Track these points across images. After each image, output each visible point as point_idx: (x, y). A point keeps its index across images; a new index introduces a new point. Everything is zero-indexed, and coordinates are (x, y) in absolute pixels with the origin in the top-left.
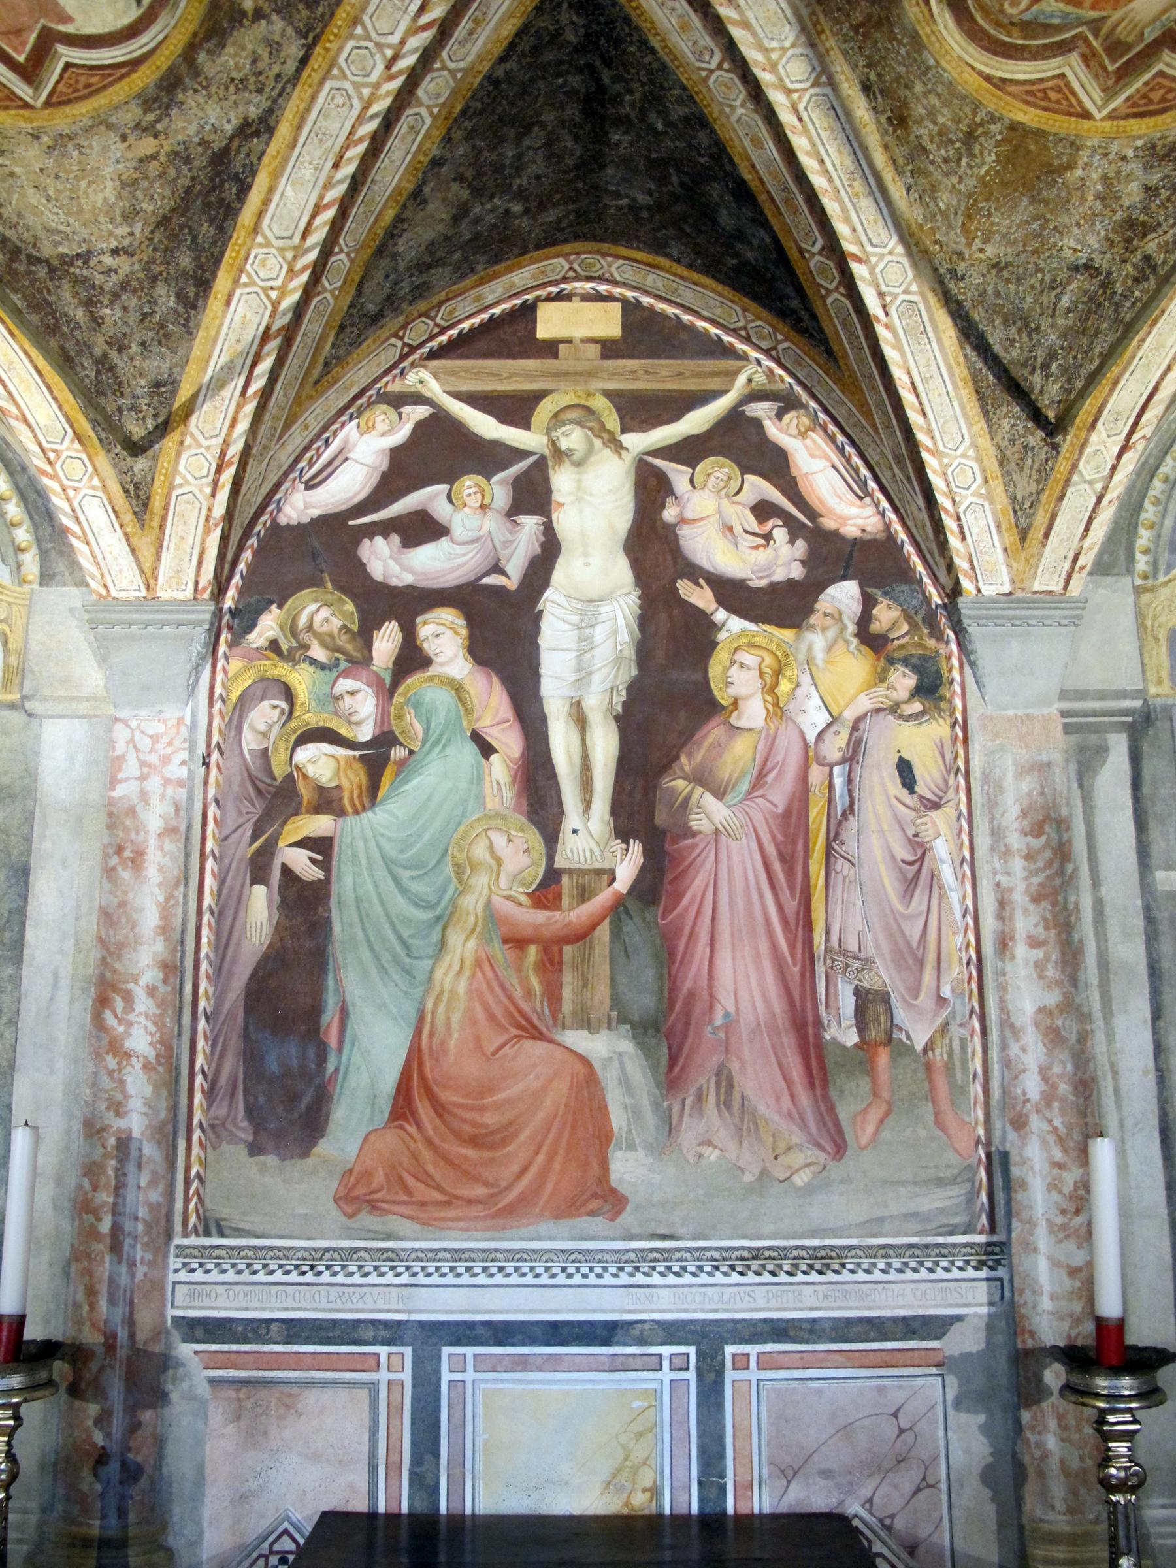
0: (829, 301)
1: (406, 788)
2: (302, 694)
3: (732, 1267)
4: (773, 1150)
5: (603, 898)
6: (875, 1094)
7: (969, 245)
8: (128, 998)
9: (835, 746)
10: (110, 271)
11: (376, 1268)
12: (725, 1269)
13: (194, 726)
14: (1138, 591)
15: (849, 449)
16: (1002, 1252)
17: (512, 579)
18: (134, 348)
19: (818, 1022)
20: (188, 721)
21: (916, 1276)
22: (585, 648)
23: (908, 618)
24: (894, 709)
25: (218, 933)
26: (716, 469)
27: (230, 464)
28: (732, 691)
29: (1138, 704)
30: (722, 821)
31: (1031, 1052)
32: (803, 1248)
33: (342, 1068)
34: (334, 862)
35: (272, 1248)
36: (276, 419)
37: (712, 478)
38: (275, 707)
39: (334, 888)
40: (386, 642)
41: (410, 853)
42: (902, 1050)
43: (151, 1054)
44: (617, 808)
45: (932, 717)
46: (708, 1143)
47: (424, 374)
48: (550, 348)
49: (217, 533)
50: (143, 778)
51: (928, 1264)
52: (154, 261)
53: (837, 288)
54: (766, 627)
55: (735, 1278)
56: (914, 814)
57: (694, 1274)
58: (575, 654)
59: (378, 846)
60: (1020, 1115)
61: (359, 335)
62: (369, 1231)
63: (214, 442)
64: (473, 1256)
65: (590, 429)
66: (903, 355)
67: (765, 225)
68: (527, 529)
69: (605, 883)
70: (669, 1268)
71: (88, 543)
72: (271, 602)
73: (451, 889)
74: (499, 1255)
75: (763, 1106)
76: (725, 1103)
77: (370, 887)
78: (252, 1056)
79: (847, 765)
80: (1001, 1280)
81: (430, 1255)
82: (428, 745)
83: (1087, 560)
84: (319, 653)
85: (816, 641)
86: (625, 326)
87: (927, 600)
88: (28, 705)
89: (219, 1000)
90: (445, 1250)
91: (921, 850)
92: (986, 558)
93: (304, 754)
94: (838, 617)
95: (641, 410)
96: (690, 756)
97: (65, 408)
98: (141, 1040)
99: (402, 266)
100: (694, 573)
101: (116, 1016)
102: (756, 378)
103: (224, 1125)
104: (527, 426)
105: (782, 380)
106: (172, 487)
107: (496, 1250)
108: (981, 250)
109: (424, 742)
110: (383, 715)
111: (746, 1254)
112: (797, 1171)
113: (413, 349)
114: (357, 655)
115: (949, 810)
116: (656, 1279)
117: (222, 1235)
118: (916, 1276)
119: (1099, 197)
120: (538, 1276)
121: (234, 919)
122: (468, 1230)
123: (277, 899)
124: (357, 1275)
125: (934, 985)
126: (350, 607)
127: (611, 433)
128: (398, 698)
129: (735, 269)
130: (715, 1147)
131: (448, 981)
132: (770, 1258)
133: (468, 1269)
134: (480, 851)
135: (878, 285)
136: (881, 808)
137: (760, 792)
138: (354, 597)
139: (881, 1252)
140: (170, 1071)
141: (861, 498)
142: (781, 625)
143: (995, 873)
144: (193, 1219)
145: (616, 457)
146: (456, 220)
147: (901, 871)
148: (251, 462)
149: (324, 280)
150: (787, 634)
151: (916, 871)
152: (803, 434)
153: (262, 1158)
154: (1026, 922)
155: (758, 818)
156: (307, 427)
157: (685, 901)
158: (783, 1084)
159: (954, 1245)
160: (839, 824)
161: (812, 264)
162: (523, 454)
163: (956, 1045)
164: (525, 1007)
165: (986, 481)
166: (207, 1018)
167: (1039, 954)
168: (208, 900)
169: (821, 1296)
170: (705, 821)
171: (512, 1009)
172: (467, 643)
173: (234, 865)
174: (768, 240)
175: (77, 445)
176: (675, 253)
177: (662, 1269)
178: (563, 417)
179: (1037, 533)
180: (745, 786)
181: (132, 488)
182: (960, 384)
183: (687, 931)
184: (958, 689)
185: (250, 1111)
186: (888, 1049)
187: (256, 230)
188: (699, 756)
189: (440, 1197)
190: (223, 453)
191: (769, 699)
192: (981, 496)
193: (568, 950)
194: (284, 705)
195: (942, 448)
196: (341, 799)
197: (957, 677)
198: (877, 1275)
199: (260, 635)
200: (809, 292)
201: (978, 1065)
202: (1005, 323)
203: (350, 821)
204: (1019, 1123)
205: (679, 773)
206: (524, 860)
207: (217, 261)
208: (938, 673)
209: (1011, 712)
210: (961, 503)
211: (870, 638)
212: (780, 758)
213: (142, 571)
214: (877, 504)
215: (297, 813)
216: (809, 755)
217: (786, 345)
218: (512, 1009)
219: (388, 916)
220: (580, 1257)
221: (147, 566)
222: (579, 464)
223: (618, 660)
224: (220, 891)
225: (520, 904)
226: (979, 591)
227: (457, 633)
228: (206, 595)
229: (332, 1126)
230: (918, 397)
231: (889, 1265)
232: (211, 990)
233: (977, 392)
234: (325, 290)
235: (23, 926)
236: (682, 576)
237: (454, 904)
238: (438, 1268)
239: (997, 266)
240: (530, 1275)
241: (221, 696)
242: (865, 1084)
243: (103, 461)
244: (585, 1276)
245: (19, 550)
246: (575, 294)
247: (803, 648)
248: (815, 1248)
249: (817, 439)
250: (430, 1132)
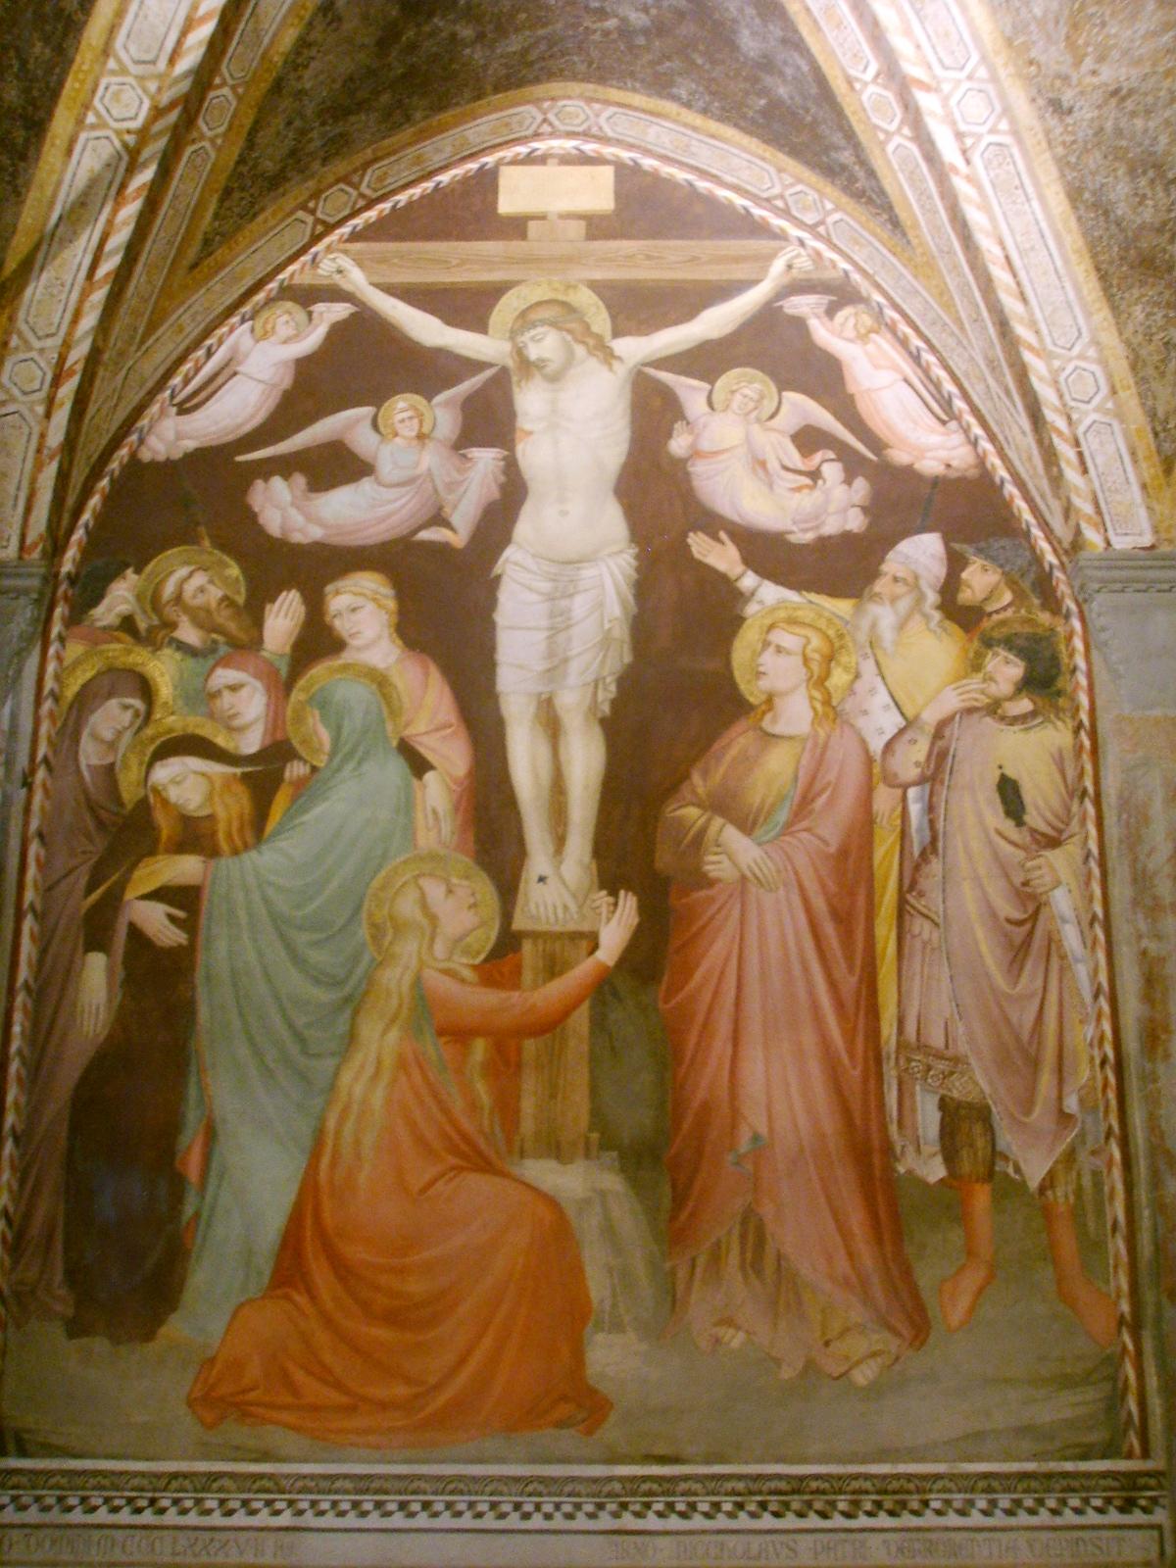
0: (890, 148)
1: (306, 818)
2: (165, 690)
3: (763, 1505)
4: (824, 1333)
5: (582, 971)
6: (970, 1252)
7: (1078, 64)
9: (911, 759)
11: (245, 1503)
12: (752, 1507)
15: (928, 357)
16: (1161, 1487)
17: (458, 536)
19: (888, 1149)
21: (1033, 1520)
22: (559, 625)
23: (1012, 584)
24: (993, 709)
26: (745, 385)
27: (71, 373)
28: (764, 684)
30: (753, 867)
32: (867, 1477)
33: (205, 1214)
34: (203, 921)
36: (136, 314)
37: (738, 397)
38: (126, 707)
39: (201, 957)
40: (283, 618)
41: (312, 907)
42: (1008, 1189)
44: (601, 848)
45: (1047, 720)
46: (729, 1322)
47: (345, 262)
48: (517, 226)
49: (51, 470)
51: (1051, 1503)
53: (899, 129)
54: (813, 597)
55: (767, 1521)
56: (1021, 854)
57: (707, 1515)
58: (545, 634)
59: (266, 901)
61: (252, 204)
62: (237, 1448)
63: (49, 342)
64: (387, 1485)
65: (569, 331)
66: (992, 218)
67: (797, 44)
68: (481, 466)
69: (584, 953)
70: (670, 1506)
72: (127, 566)
73: (366, 960)
74: (423, 1485)
75: (809, 1267)
76: (754, 1265)
77: (251, 956)
78: (78, 1193)
79: (927, 787)
80: (1159, 1527)
81: (324, 1484)
82: (339, 757)
84: (189, 633)
85: (883, 616)
86: (618, 195)
87: (1037, 559)
89: (33, 1113)
90: (346, 1477)
91: (1032, 904)
92: (1118, 497)
93: (162, 773)
94: (914, 584)
95: (639, 306)
96: (705, 774)
99: (310, 109)
100: (712, 523)
102: (797, 263)
103: (33, 1292)
104: (480, 325)
105: (834, 266)
107: (420, 1477)
108: (1094, 73)
109: (333, 754)
110: (276, 717)
111: (783, 1485)
112: (858, 1363)
113: (330, 228)
114: (242, 636)
115: (1072, 849)
116: (652, 1522)
118: (1033, 1520)
120: (479, 1515)
122: (378, 1447)
123: (120, 973)
124: (217, 1514)
125: (1054, 1094)
126: (234, 571)
127: (599, 338)
128: (297, 695)
129: (765, 113)
130: (738, 1328)
131: (358, 1090)
132: (818, 1492)
133: (378, 1505)
134: (407, 907)
135: (953, 123)
136: (976, 845)
137: (805, 824)
138: (240, 557)
139: (982, 1484)
141: (944, 423)
142: (834, 592)
143: (1140, 937)
145: (604, 369)
146: (383, 44)
147: (1006, 935)
148: (101, 372)
149: (200, 122)
150: (843, 607)
151: (1026, 934)
152: (863, 338)
153: (85, 1340)
155: (802, 861)
156: (181, 330)
157: (698, 976)
158: (838, 1239)
159: (1087, 1475)
160: (917, 868)
161: (865, 97)
162: (477, 366)
163: (1087, 1181)
164: (467, 1125)
165: (1114, 391)
166: (17, 1140)
168: (24, 973)
169: (893, 1549)
170: (726, 863)
171: (448, 1128)
172: (395, 619)
173: (63, 922)
174: (805, 68)
176: (683, 94)
177: (659, 1507)
178: (533, 316)
180: (782, 816)
182: (1073, 258)
183: (700, 1018)
184: (1083, 681)
185: (72, 1275)
186: (987, 1188)
187: (106, 51)
188: (718, 775)
189: (337, 1398)
190: (62, 359)
191: (817, 694)
192: (1107, 412)
193: (530, 1046)
194: (138, 703)
195: (1050, 347)
196: (214, 834)
197: (1081, 663)
198: (976, 1519)
199: (109, 610)
202: (1132, 172)
203: (226, 864)
205: (689, 796)
206: (468, 919)
207: (54, 94)
208: (1055, 660)
209: (1158, 712)
210: (1080, 421)
211: (959, 613)
212: (831, 777)
214: (966, 431)
216: (874, 771)
217: (837, 216)
218: (448, 1128)
219: (277, 998)
220: (541, 1488)
222: (554, 378)
223: (606, 641)
224: (41, 961)
225: (463, 981)
226: (1108, 543)
227: (380, 606)
228: (36, 555)
229: (188, 1296)
230: (1015, 276)
231: (993, 1503)
232: (23, 1100)
233: (1098, 269)
234: (202, 137)
236: (695, 528)
237: (369, 980)
238: (335, 1504)
240: (468, 1515)
241: (52, 693)
242: (956, 1236)
244: (548, 1517)
246: (552, 156)
247: (865, 624)
248: (884, 1477)
249: (883, 343)
250: (329, 1305)
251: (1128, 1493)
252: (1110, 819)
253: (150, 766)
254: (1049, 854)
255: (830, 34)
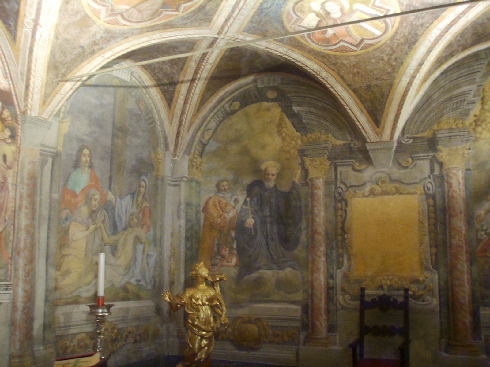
0: (25, 29)
14: (60, 122)
15: (5, 64)
23: (11, 116)
24: (4, 140)
29: (55, 151)
31: (23, 235)
60: (19, 252)
80: (10, 293)
83: (54, 113)
87: (16, 112)
119: (93, 35)
154: (25, 203)
163: (7, 233)
167: (27, 211)
179: (47, 103)
200: (20, 23)
201: (11, 238)
204: (18, 254)
214: (8, 81)
239: (66, 40)
251: (7, 287)
252: (19, 166)
254: (9, 170)
255: (28, 7)
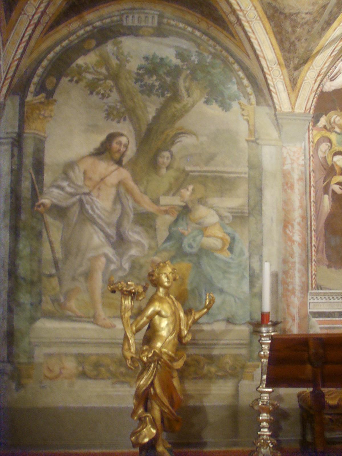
8: (293, 226)
10: (303, 18)
13: (305, 149)
18: (303, 40)
20: (303, 147)
25: (316, 208)
35: (335, 293)
38: (327, 145)
43: (300, 241)
50: (292, 164)
52: (317, 17)
71: (277, 95)
78: (327, 242)
84: (337, 130)
88: (258, 141)
89: (317, 226)
97: (278, 55)
98: (297, 237)
101: (289, 231)
106: (303, 80)
117: (321, 289)
121: (320, 204)
123: (331, 199)
140: (306, 246)
144: (314, 285)
166: (314, 231)
168: (312, 199)
175: (278, 66)
181: (292, 80)
185: (328, 257)
190: (320, 72)
194: (329, 144)
207: (335, 18)
213: (291, 104)
215: (335, 175)
221: (293, 102)
224: (316, 196)
232: (315, 224)
235: (261, 205)
241: (312, 141)
243: (285, 71)
245: (249, 94)
253: (333, 157)
